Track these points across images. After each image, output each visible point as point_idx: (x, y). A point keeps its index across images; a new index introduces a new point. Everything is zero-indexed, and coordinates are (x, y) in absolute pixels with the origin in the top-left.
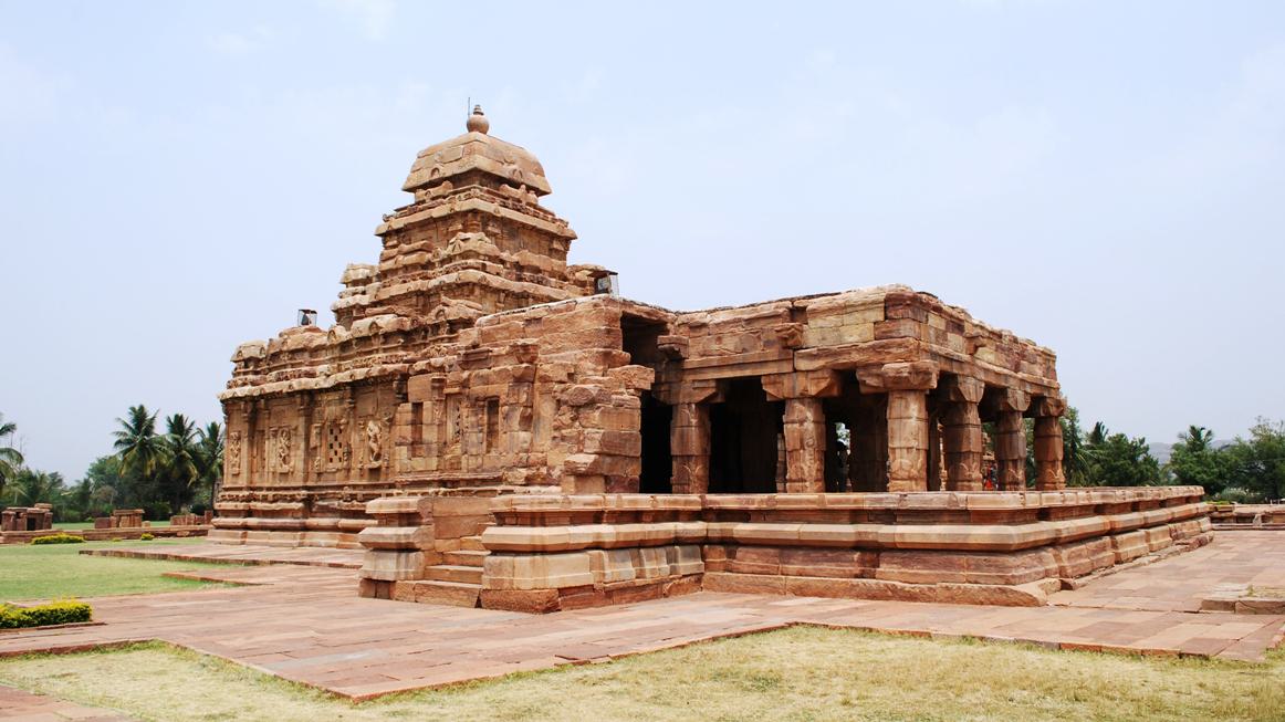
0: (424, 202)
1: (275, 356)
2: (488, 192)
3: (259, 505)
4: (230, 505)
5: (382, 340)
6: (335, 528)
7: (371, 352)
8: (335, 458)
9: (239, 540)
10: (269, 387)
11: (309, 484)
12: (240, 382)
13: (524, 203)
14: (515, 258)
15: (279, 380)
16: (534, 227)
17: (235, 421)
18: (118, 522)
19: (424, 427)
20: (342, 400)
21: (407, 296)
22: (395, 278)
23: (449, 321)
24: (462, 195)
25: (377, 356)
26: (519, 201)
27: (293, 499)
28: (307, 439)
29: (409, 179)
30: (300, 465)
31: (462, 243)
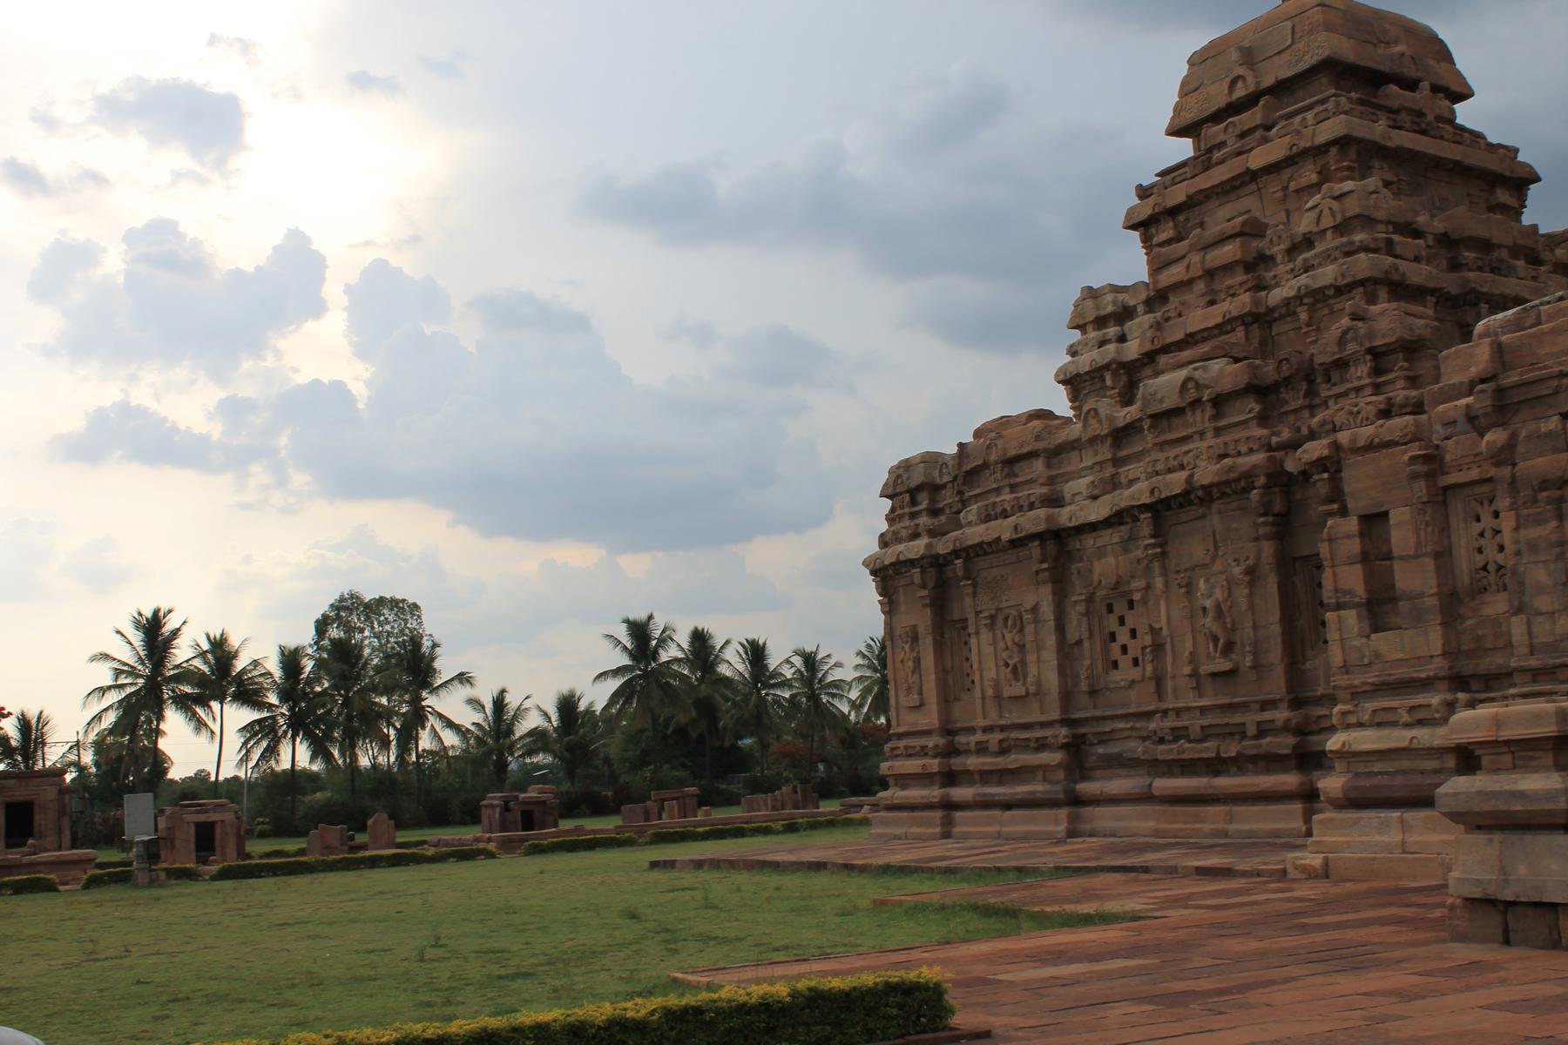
0: (1223, 144)
1: (972, 475)
2: (1361, 102)
3: (973, 762)
4: (913, 765)
5: (1209, 411)
6: (1146, 798)
8: (1125, 661)
10: (975, 533)
11: (1170, 704)
12: (904, 533)
13: (1430, 117)
14: (1439, 225)
15: (988, 518)
16: (1457, 163)
17: (903, 608)
18: (661, 809)
19: (1397, 565)
20: (1127, 543)
21: (1222, 328)
22: (1188, 297)
23: (1370, 351)
24: (1309, 116)
25: (1204, 444)
26: (1421, 114)
27: (1042, 745)
28: (1061, 628)
29: (1178, 109)
30: (1052, 679)
31: (1335, 205)
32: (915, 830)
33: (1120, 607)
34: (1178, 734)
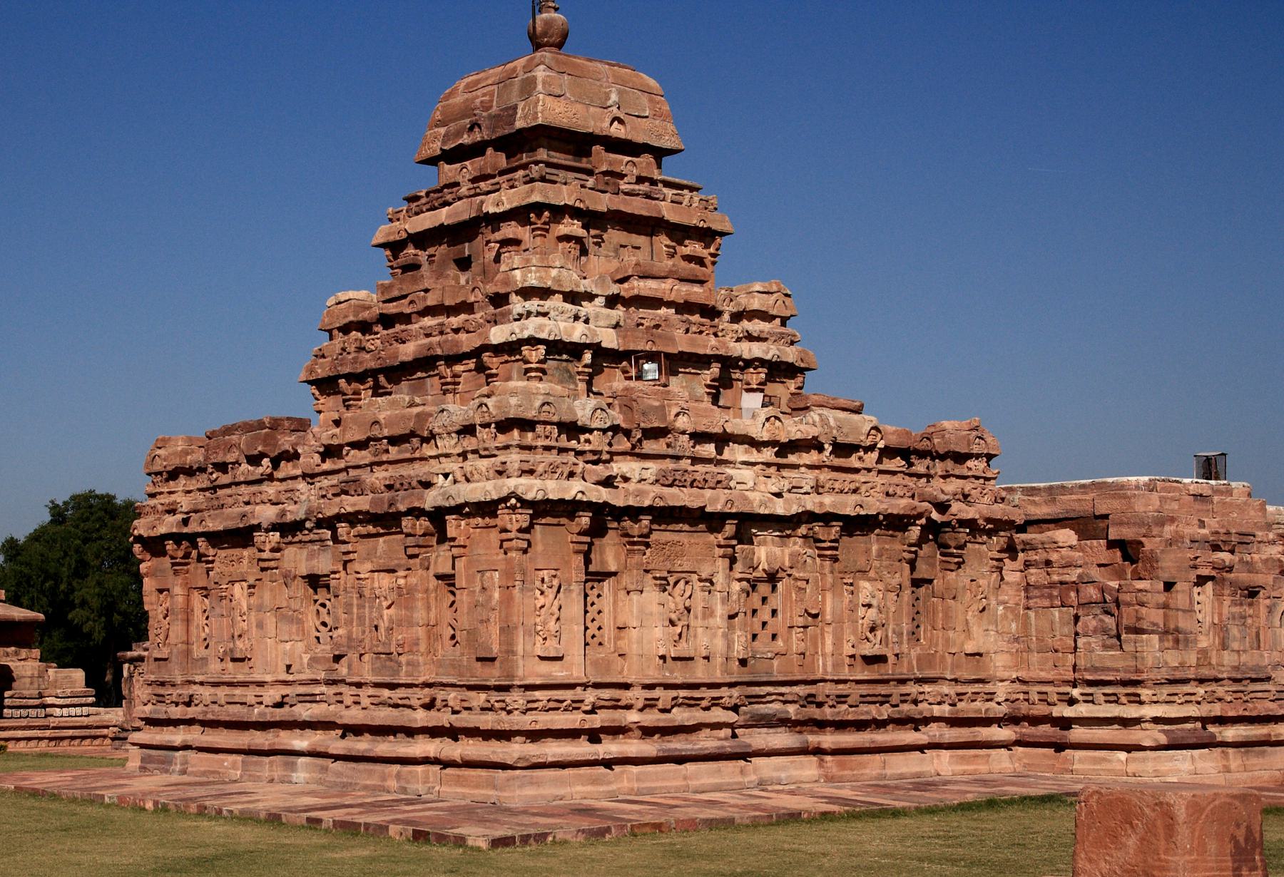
7: (857, 471)
32: (579, 788)
33: (764, 588)
34: (841, 698)
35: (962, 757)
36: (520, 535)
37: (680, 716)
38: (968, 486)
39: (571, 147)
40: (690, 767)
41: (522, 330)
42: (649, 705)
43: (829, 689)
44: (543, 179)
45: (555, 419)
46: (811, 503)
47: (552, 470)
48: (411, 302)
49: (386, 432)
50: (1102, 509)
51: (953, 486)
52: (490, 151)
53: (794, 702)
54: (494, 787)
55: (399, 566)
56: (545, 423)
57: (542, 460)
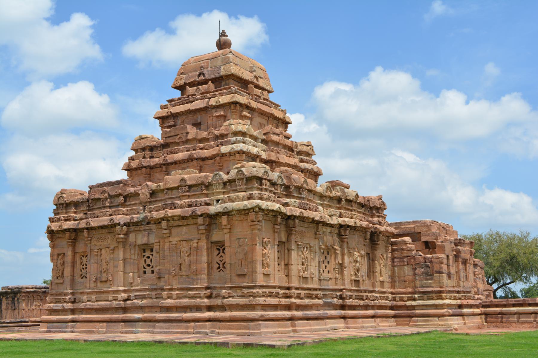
7: (351, 210)
8: (326, 271)
9: (291, 329)
27: (317, 297)
32: (280, 329)
35: (382, 321)
36: (259, 223)
37: (307, 301)
38: (381, 219)
39: (239, 84)
40: (312, 322)
41: (236, 147)
42: (299, 297)
43: (349, 293)
44: (236, 93)
45: (268, 178)
46: (340, 220)
47: (268, 199)
48: (180, 138)
49: (189, 183)
50: (418, 230)
51: (376, 219)
52: (210, 83)
53: (336, 298)
54: (249, 329)
55: (195, 238)
56: (265, 179)
57: (266, 194)
